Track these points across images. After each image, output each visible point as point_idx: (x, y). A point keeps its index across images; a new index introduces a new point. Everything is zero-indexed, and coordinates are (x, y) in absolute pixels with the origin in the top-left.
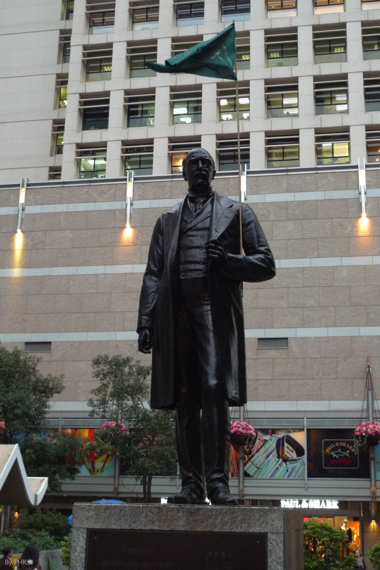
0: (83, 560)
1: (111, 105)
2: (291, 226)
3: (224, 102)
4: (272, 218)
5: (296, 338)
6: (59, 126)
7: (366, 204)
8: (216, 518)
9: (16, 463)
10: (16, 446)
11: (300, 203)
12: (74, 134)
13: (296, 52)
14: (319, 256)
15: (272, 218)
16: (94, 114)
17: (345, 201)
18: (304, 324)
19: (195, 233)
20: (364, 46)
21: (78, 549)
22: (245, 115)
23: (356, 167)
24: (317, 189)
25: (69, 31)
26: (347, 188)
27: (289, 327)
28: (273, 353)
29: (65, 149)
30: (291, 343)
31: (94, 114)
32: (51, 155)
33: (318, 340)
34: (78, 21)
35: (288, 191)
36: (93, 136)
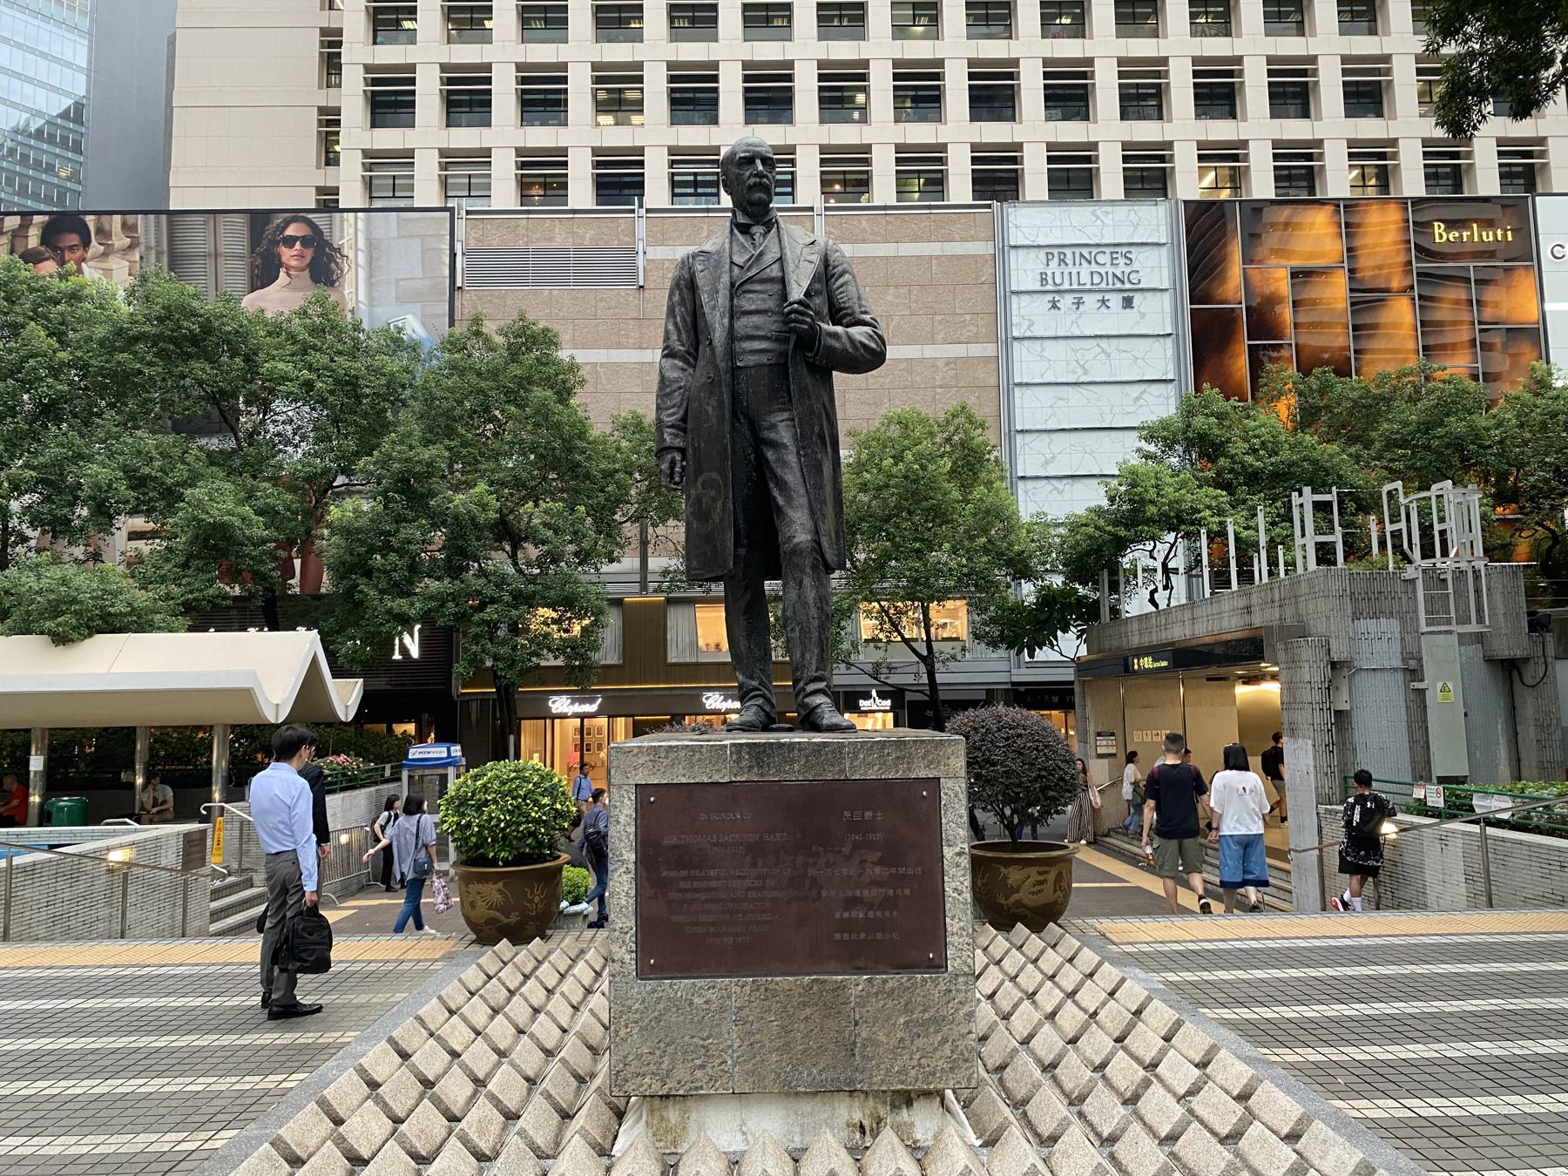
0: (632, 837)
3: (602, 96)
6: (330, 120)
8: (856, 757)
9: (314, 662)
12: (356, 133)
13: (715, 20)
16: (390, 100)
19: (758, 287)
20: (820, 19)
21: (622, 819)
22: (636, 119)
23: (811, 209)
31: (390, 100)
32: (318, 167)
36: (389, 138)
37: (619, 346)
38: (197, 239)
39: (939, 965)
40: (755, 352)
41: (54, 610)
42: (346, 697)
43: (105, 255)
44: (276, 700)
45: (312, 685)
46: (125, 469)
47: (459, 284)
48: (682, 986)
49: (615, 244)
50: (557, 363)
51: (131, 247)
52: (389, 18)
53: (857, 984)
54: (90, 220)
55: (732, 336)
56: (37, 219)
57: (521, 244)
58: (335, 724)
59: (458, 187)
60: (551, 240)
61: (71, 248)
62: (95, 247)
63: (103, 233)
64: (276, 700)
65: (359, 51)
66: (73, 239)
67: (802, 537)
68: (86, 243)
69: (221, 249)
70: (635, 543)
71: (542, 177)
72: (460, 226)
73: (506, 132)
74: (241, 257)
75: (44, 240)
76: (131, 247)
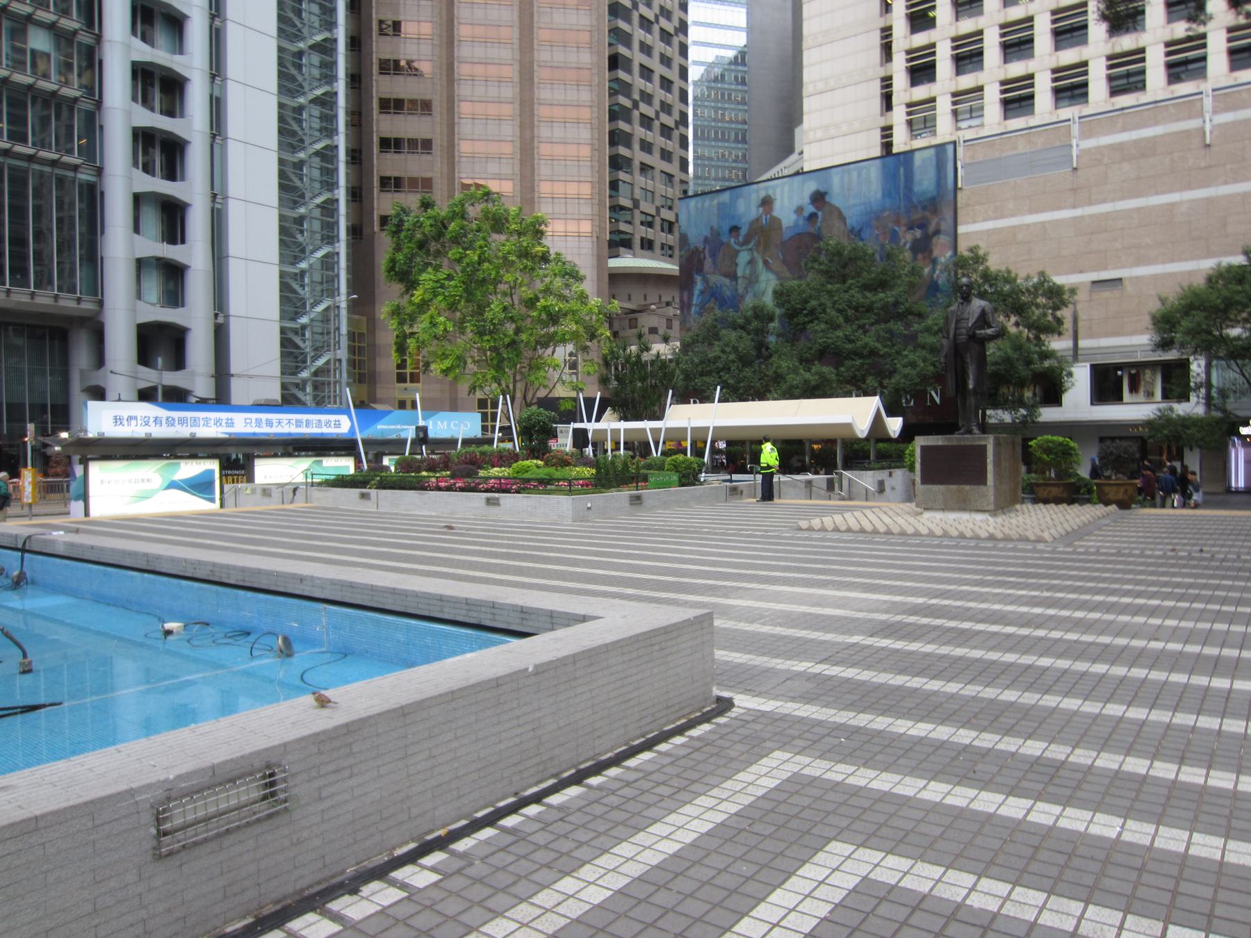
1: (938, 57)
2: (1126, 167)
4: (1106, 160)
5: (1131, 279)
7: (1211, 132)
9: (878, 412)
10: (877, 398)
11: (1136, 142)
14: (1157, 193)
15: (1106, 160)
17: (1187, 134)
18: (1139, 262)
24: (1156, 123)
25: (890, 28)
26: (1190, 117)
27: (1123, 267)
28: (1106, 294)
29: (895, 57)
30: (1126, 283)
31: (922, 71)
33: (1155, 277)
34: (899, 19)
35: (1124, 130)
36: (921, 92)
37: (1059, 208)
39: (985, 484)
40: (963, 338)
42: (895, 425)
44: (862, 428)
45: (877, 422)
47: (959, 185)
48: (931, 487)
49: (1057, 144)
50: (970, 278)
52: (920, 19)
53: (967, 487)
55: (955, 335)
57: (997, 155)
58: (889, 440)
59: (964, 112)
60: (1015, 149)
64: (862, 428)
65: (903, 39)
67: (971, 387)
70: (1071, 332)
71: (1017, 99)
72: (960, 151)
73: (995, 69)
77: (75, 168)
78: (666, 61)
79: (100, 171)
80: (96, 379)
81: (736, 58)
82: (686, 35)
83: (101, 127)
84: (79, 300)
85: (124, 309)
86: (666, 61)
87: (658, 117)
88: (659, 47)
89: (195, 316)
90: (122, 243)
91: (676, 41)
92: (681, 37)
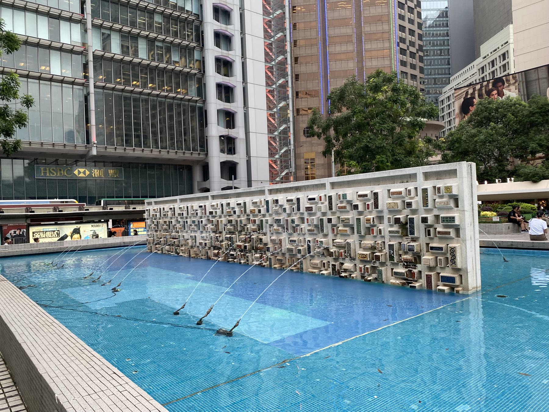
38: (533, 76)
41: (534, 176)
43: (509, 86)
46: (537, 144)
51: (515, 82)
54: (504, 78)
56: (491, 81)
61: (500, 86)
62: (506, 84)
63: (508, 81)
66: (500, 84)
68: (504, 84)
69: (540, 77)
74: (546, 78)
75: (493, 86)
76: (515, 82)
77: (196, 101)
78: (411, 21)
79: (204, 102)
80: (205, 185)
81: (440, 15)
82: (420, 7)
83: (205, 84)
84: (199, 154)
85: (216, 157)
86: (411, 21)
87: (408, 49)
88: (408, 15)
89: (239, 158)
90: (215, 130)
91: (415, 11)
92: (418, 9)
